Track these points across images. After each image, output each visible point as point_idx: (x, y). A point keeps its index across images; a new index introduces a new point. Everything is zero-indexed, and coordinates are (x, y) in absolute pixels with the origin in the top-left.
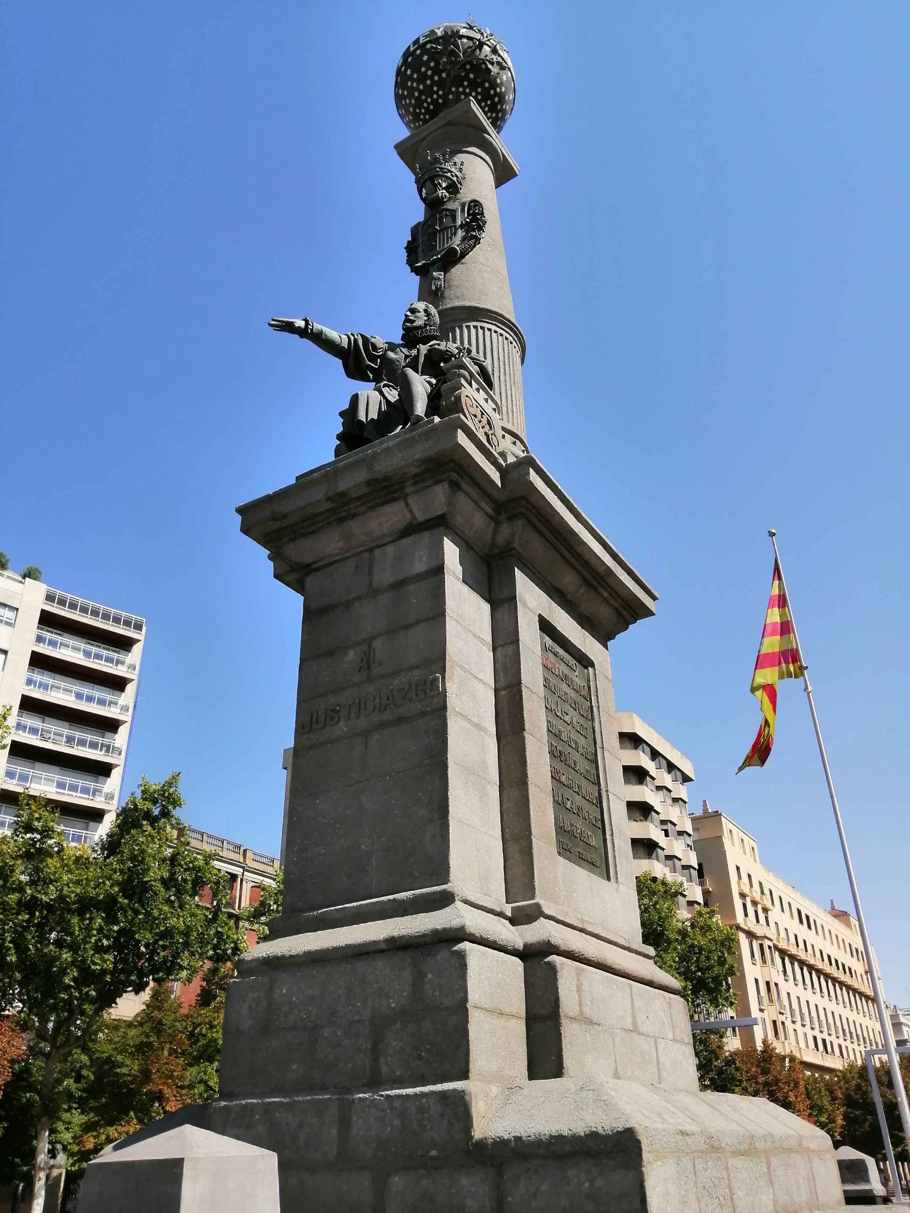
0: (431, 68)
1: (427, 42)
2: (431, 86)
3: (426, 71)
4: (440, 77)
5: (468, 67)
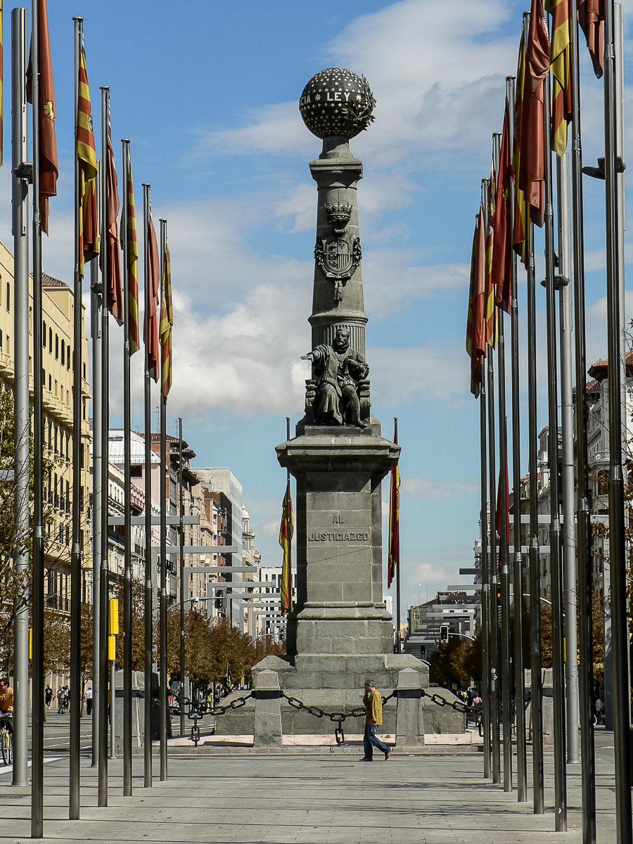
1: (339, 102)
3: (335, 119)
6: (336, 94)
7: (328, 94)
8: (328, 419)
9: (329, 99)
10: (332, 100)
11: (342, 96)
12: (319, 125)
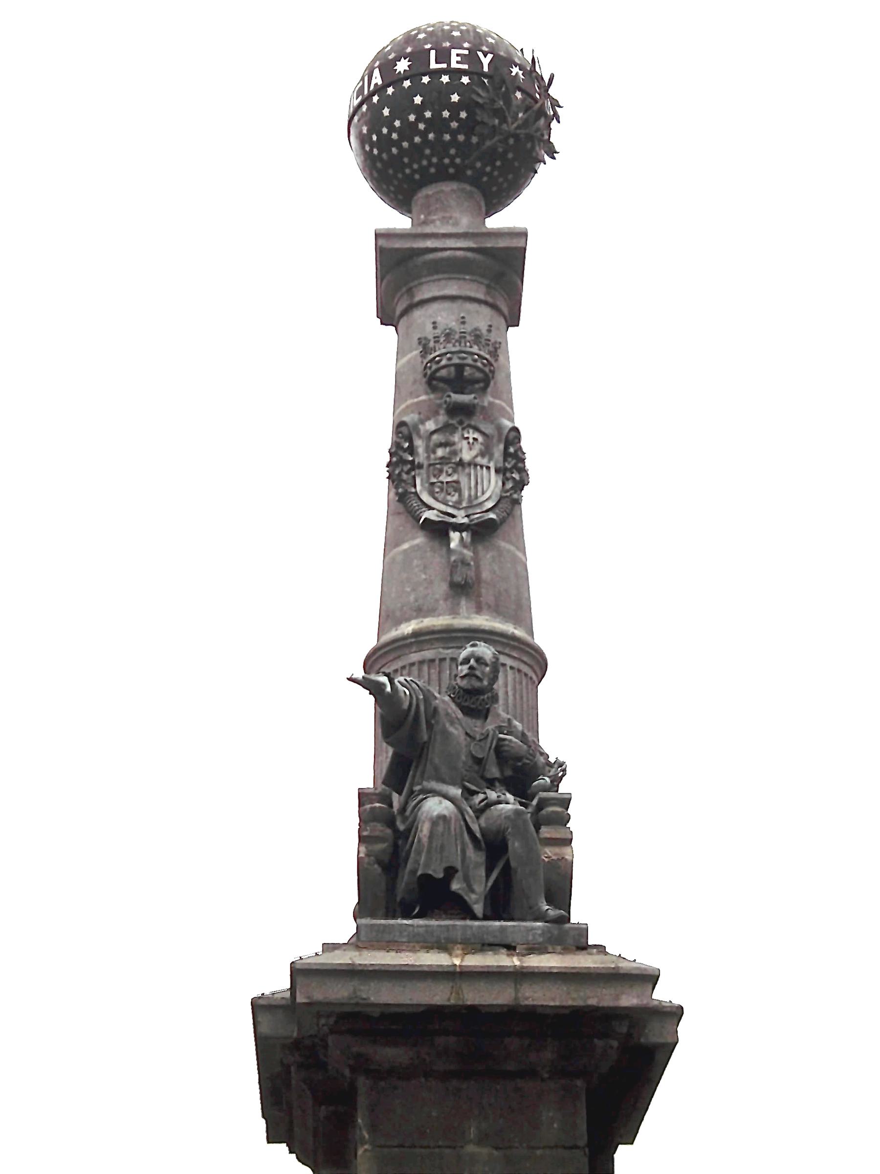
0: (459, 120)
2: (446, 146)
4: (468, 138)
5: (511, 141)
6: (454, 52)
7: (433, 53)
8: (434, 897)
9: (433, 65)
10: (444, 66)
11: (472, 58)
12: (408, 171)
